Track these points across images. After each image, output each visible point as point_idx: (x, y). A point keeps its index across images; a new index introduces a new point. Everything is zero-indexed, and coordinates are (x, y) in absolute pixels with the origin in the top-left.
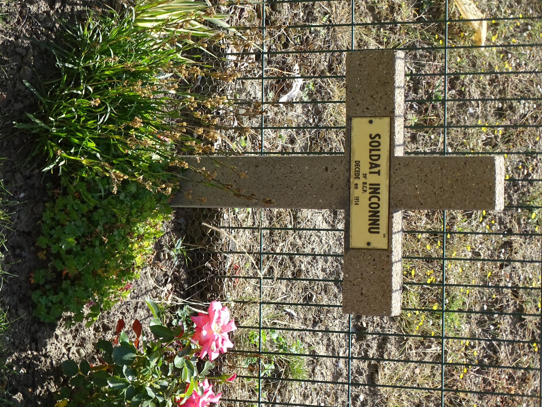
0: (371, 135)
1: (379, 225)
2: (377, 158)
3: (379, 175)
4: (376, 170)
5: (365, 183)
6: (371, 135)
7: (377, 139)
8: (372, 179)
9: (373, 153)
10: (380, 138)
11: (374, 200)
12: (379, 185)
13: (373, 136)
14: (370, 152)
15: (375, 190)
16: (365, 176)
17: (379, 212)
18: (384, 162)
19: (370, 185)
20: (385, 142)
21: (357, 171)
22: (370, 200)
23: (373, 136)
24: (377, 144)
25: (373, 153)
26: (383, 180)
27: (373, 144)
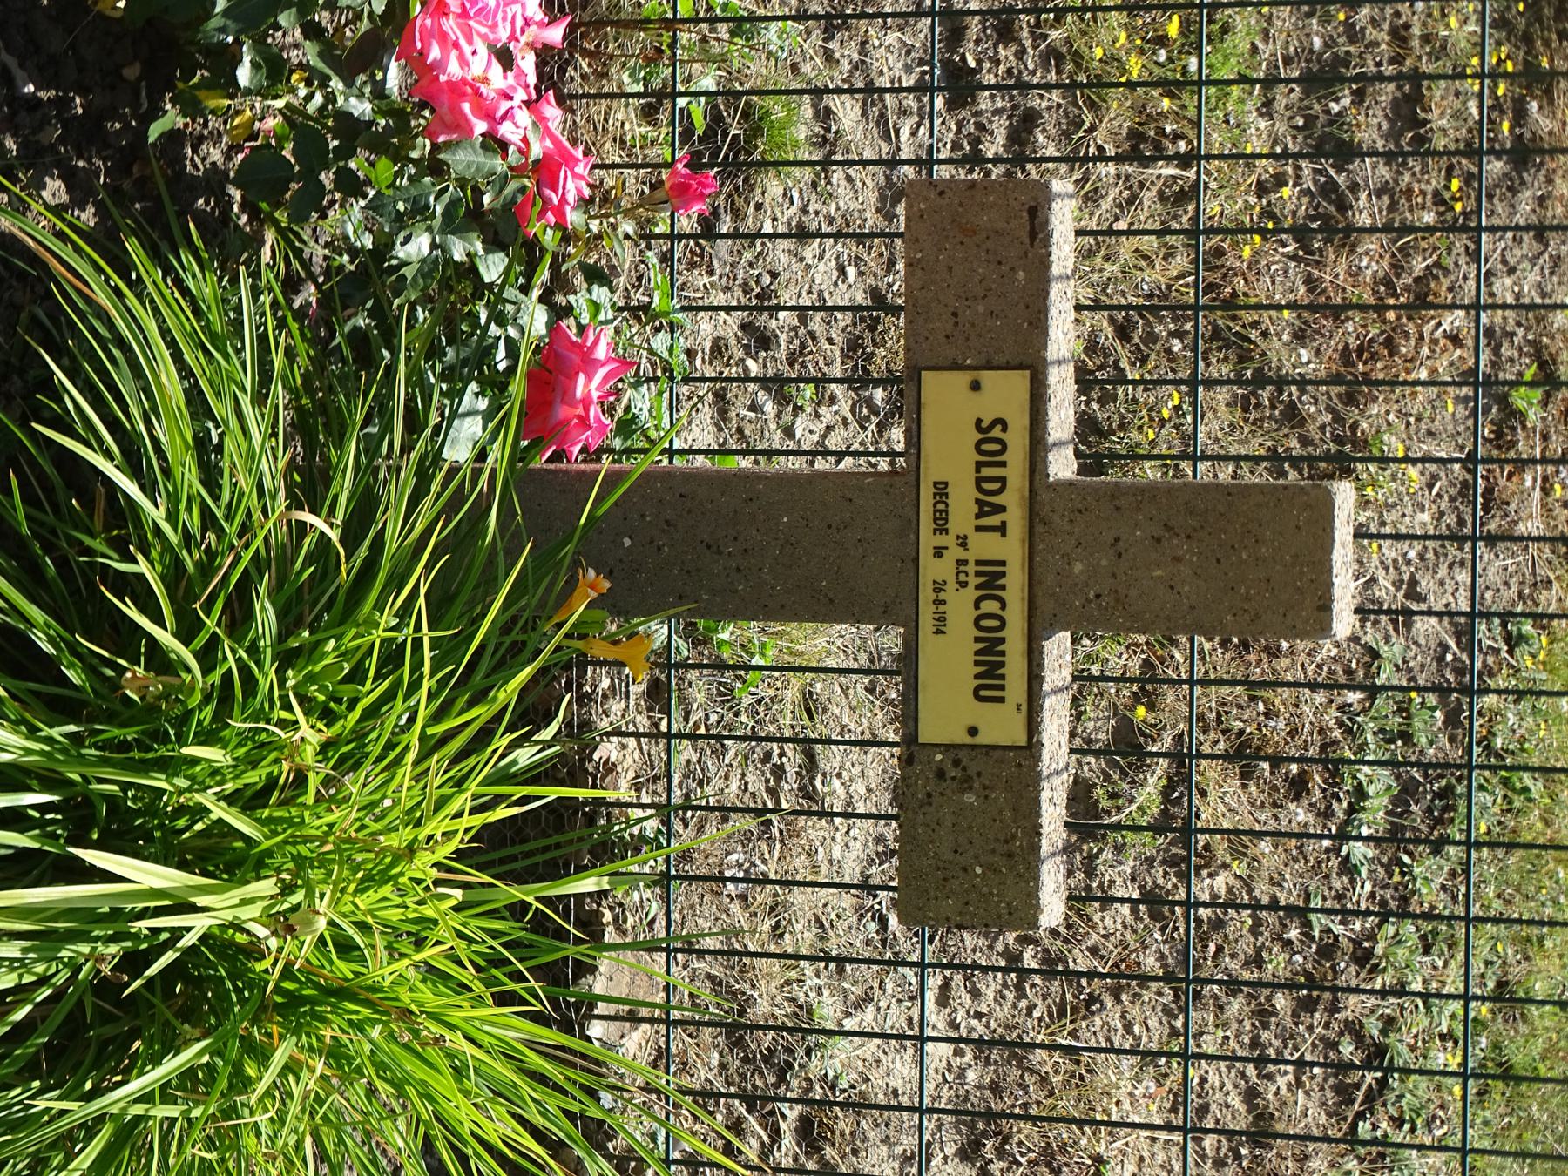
0: (979, 421)
1: (1003, 677)
2: (996, 486)
3: (1004, 535)
4: (994, 520)
5: (965, 562)
6: (979, 421)
7: (996, 432)
8: (986, 546)
9: (987, 472)
10: (1004, 430)
11: (990, 606)
12: (1003, 563)
13: (984, 425)
14: (978, 471)
15: (991, 578)
16: (963, 542)
17: (1003, 640)
18: (1013, 501)
19: (978, 563)
20: (1017, 440)
21: (941, 511)
22: (977, 607)
23: (984, 425)
24: (996, 447)
25: (987, 472)
26: (1010, 549)
27: (985, 447)
